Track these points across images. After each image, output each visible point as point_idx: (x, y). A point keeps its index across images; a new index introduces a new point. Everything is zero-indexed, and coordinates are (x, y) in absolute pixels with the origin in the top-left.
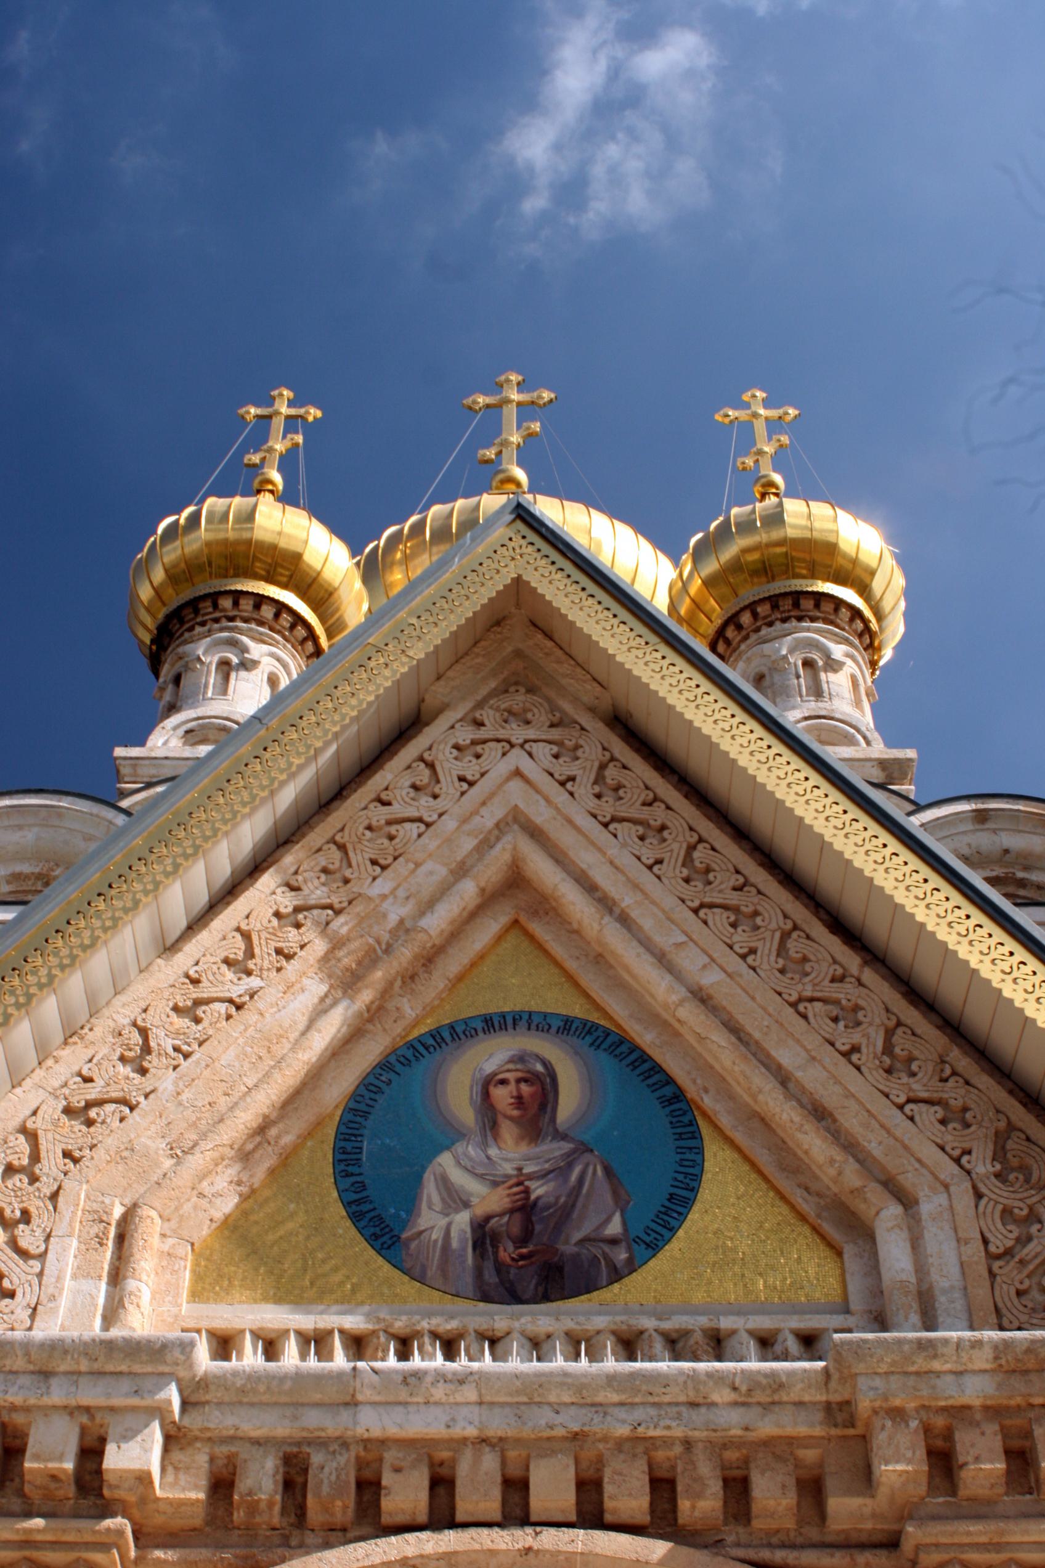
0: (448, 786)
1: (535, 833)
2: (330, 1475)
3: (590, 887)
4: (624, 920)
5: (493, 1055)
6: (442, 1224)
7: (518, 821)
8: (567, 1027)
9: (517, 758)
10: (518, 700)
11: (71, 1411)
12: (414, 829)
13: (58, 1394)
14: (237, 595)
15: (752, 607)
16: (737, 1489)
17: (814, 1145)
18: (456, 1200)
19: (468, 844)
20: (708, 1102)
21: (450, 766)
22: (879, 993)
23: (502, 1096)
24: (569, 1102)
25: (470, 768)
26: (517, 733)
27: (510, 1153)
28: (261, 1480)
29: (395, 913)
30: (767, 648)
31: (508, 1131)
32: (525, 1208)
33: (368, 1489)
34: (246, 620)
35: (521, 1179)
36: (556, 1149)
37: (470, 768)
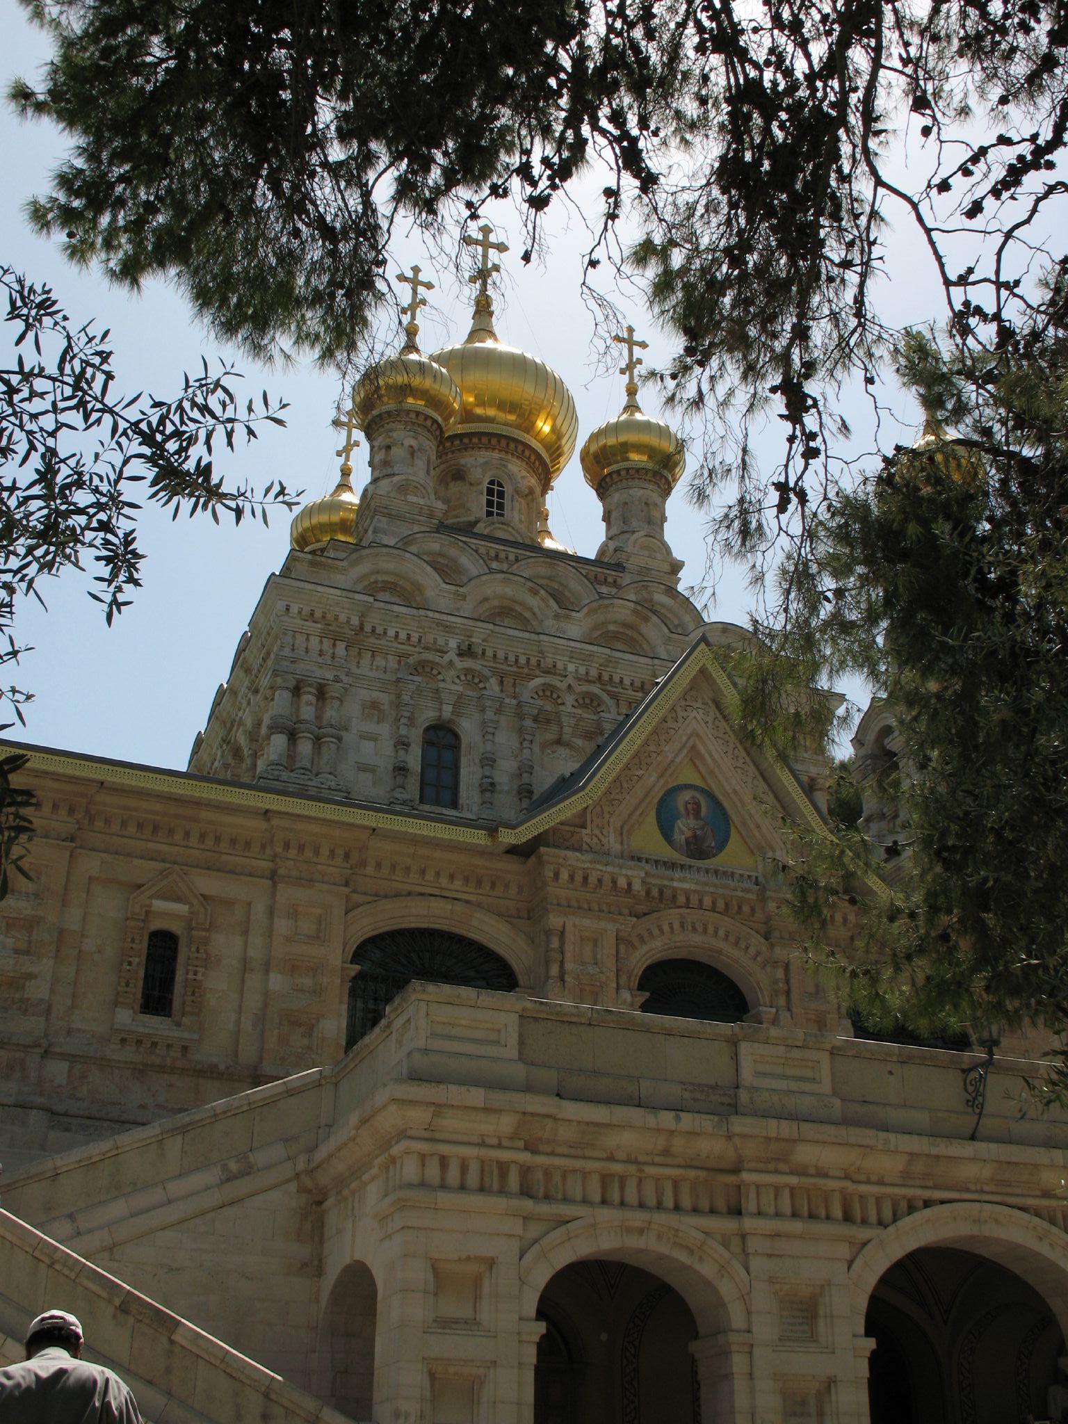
0: (680, 720)
1: (698, 736)
2: (668, 893)
3: (711, 755)
4: (719, 766)
5: (687, 796)
6: (680, 838)
7: (694, 734)
8: (702, 791)
9: (695, 713)
10: (693, 693)
11: (626, 876)
12: (672, 732)
13: (624, 872)
14: (418, 414)
15: (628, 470)
16: (740, 907)
17: (757, 834)
18: (682, 833)
19: (685, 738)
20: (734, 817)
21: (681, 713)
22: (770, 798)
23: (690, 806)
24: (704, 810)
25: (685, 714)
26: (695, 705)
27: (692, 822)
28: (655, 893)
29: (670, 756)
30: (631, 491)
31: (691, 817)
32: (695, 836)
33: (674, 897)
34: (419, 425)
35: (694, 829)
36: (701, 823)
37: (685, 714)
